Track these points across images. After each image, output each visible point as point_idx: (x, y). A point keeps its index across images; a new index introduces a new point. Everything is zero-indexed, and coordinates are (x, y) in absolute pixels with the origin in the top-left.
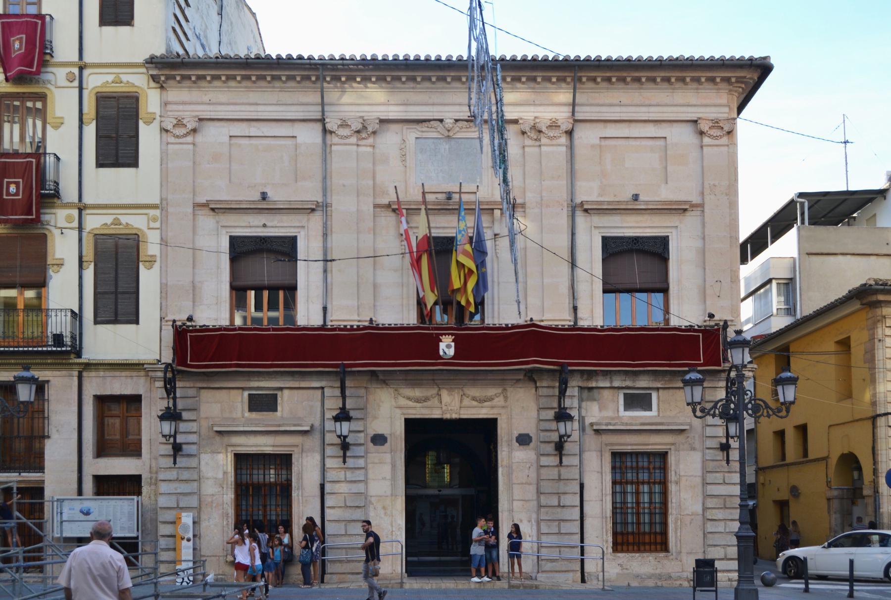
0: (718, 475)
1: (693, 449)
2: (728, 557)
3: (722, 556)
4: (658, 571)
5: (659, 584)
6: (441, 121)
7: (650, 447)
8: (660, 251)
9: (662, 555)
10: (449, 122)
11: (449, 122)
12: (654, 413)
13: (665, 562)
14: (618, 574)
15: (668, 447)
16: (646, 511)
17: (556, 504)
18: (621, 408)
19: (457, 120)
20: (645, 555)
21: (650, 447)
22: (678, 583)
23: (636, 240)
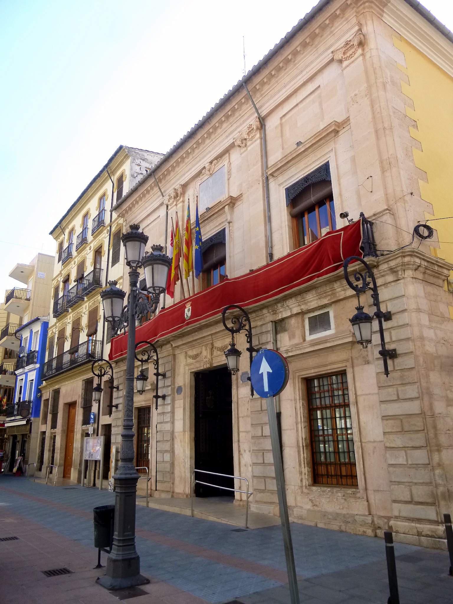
0: (390, 390)
1: (368, 362)
2: (416, 499)
3: (408, 498)
4: (344, 512)
5: (343, 528)
6: (204, 168)
7: (329, 368)
8: (324, 177)
9: (350, 491)
10: (207, 165)
11: (207, 165)
12: (331, 332)
13: (352, 500)
14: (309, 510)
15: (344, 365)
16: (331, 438)
17: (260, 434)
18: (307, 332)
19: (211, 163)
20: (335, 490)
21: (329, 368)
22: (362, 529)
23: (306, 179)
